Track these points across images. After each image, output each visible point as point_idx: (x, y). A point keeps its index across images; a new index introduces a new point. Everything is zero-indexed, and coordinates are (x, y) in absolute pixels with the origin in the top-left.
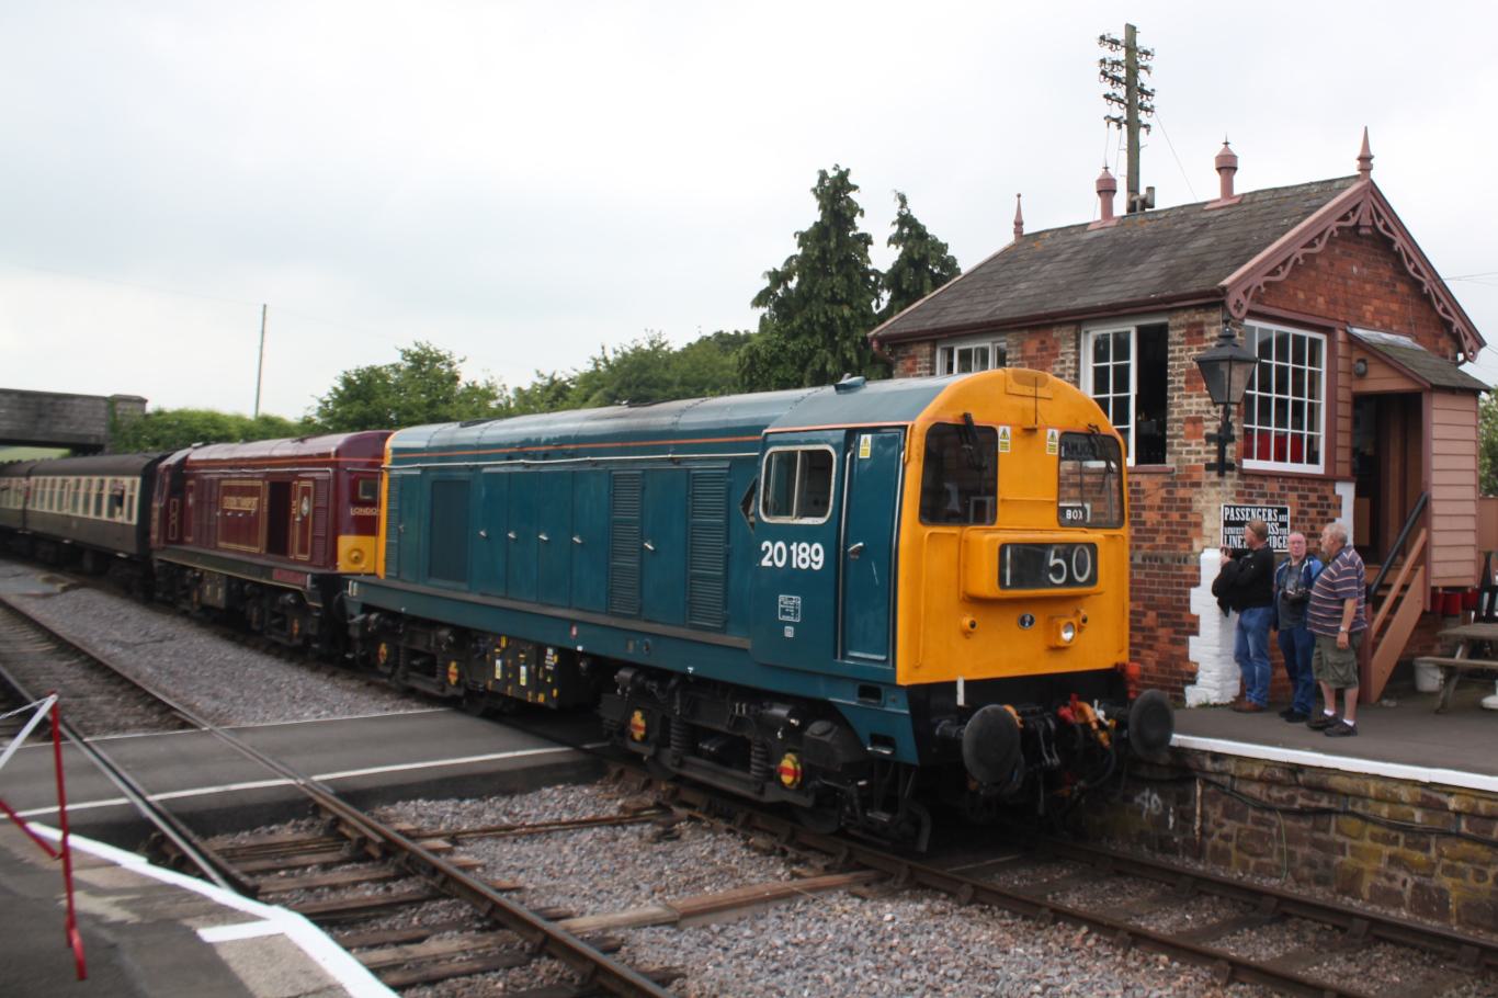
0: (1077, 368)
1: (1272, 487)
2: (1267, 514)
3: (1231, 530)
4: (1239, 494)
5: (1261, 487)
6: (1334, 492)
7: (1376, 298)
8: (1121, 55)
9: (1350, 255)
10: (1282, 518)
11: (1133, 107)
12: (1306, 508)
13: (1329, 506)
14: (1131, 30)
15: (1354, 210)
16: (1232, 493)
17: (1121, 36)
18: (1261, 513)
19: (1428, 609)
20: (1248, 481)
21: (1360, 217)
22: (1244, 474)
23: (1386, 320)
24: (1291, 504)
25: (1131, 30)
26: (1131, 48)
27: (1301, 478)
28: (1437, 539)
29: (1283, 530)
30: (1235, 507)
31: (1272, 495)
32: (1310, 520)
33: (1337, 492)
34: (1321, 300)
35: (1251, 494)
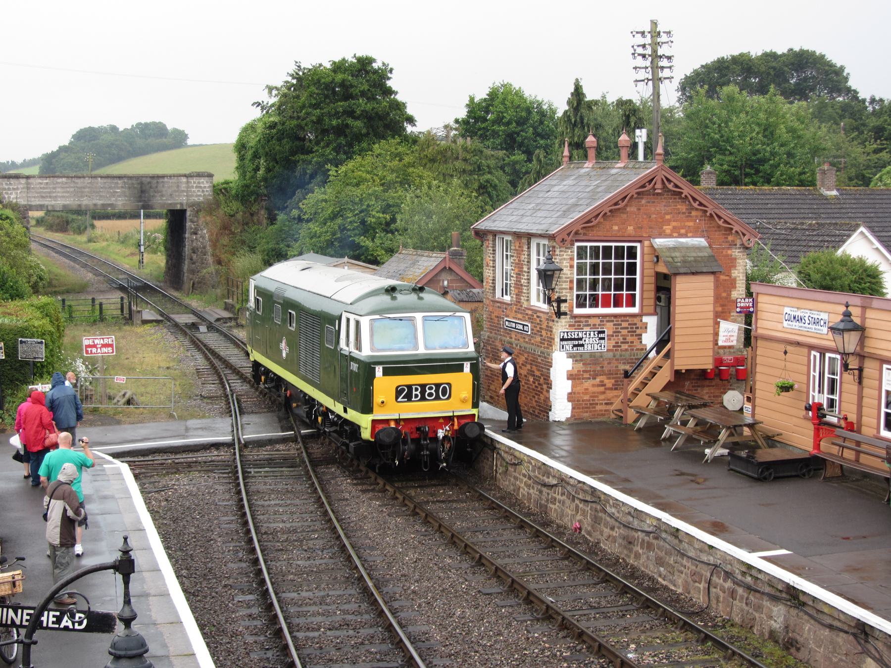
0: (529, 258)
1: (597, 321)
2: (590, 335)
3: (565, 343)
4: (570, 326)
5: (587, 321)
6: (641, 321)
7: (674, 221)
8: (648, 40)
9: (654, 202)
10: (601, 335)
11: (655, 68)
12: (619, 330)
13: (637, 328)
14: (654, 24)
15: (650, 181)
16: (565, 326)
17: (647, 28)
18: (586, 334)
19: (673, 380)
20: (577, 319)
21: (655, 184)
22: (575, 317)
23: (683, 231)
24: (607, 328)
25: (654, 24)
26: (655, 34)
27: (615, 316)
28: (677, 347)
29: (602, 341)
30: (567, 332)
31: (594, 325)
32: (622, 336)
33: (644, 321)
34: (630, 228)
35: (580, 325)
